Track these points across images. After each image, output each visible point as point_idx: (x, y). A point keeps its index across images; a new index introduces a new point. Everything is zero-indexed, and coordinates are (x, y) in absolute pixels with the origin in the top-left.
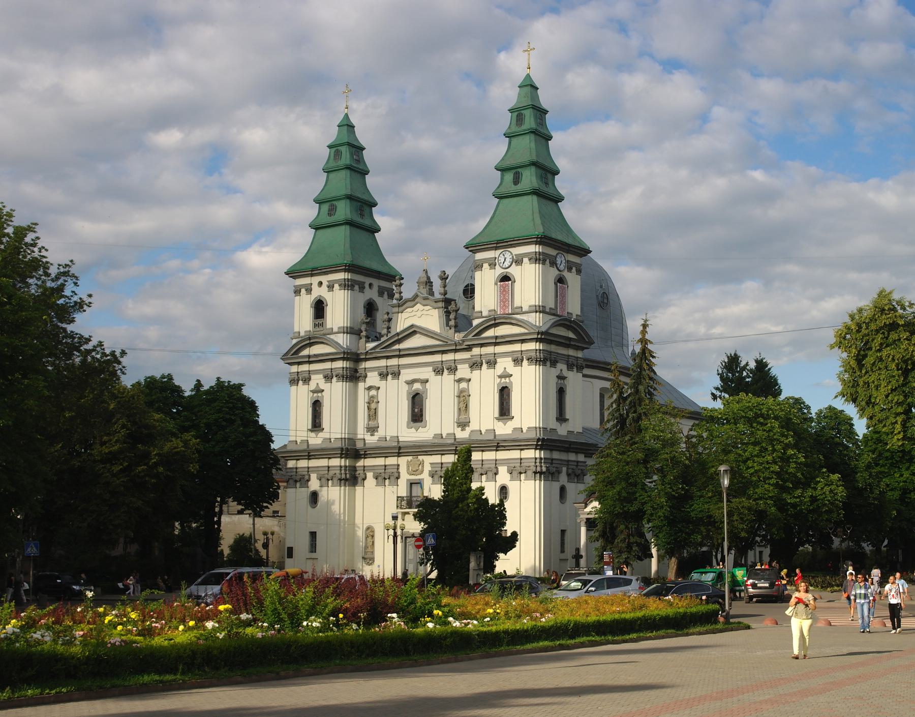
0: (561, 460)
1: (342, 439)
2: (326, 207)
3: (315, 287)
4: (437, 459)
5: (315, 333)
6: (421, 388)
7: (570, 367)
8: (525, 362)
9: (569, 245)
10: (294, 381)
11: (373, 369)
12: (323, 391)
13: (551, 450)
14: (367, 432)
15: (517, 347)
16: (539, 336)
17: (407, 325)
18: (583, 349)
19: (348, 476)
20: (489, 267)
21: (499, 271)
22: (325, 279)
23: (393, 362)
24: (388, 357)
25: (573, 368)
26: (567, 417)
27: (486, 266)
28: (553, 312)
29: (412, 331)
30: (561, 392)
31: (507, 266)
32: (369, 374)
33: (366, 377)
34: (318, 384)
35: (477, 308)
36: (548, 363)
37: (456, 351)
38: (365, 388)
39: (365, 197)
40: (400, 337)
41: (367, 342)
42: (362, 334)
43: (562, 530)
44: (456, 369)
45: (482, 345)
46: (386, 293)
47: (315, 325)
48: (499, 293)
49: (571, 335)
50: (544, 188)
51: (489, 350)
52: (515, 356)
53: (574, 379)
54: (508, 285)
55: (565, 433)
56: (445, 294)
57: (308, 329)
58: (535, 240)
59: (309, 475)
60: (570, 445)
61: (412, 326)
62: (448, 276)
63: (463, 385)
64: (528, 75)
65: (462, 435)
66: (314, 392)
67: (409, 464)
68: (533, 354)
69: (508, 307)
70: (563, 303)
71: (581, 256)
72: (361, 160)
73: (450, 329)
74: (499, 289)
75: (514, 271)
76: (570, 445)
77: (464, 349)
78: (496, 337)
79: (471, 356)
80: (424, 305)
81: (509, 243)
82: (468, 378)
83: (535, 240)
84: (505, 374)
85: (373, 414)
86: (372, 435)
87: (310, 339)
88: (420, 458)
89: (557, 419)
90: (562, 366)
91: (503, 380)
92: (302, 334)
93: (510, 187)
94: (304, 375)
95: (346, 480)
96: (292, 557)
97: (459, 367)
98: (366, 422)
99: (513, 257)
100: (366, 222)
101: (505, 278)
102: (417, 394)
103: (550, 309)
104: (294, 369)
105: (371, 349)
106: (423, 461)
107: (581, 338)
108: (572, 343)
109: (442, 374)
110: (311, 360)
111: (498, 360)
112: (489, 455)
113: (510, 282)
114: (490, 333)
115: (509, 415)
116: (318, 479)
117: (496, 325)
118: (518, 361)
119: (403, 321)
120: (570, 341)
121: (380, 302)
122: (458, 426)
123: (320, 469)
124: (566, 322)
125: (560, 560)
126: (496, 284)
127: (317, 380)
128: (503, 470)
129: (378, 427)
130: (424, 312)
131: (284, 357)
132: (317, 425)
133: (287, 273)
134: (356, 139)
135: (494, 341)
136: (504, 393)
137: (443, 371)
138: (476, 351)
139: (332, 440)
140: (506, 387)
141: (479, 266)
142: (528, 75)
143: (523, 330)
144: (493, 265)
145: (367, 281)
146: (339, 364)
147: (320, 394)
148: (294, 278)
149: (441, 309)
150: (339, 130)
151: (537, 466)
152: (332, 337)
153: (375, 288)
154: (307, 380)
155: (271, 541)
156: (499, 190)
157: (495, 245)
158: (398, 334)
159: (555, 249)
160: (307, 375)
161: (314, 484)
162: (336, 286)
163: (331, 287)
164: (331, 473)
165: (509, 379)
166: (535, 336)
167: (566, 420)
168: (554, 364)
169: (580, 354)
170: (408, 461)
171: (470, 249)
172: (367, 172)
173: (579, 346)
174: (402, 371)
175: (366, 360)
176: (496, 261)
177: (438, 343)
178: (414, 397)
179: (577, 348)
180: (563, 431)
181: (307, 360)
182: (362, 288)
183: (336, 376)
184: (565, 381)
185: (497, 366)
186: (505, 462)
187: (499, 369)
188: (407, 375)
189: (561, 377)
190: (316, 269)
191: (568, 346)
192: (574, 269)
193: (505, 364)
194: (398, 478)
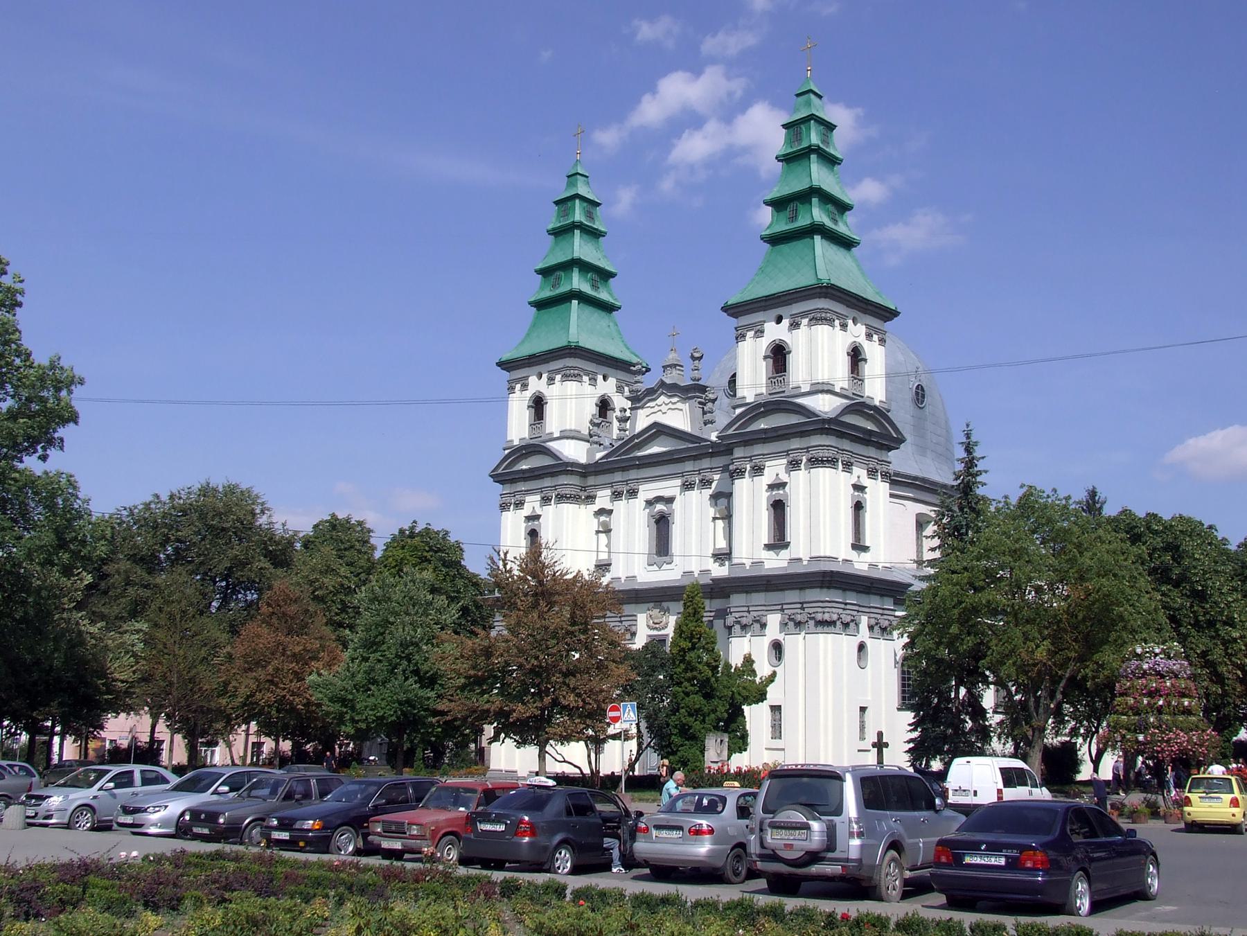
6: (665, 508)
7: (872, 473)
18: (890, 449)
26: (867, 544)
28: (844, 392)
29: (658, 430)
30: (858, 507)
33: (594, 497)
37: (712, 455)
43: (861, 707)
50: (828, 222)
53: (878, 491)
55: (865, 567)
56: (698, 380)
58: (818, 290)
61: (655, 424)
80: (671, 396)
81: (783, 299)
82: (727, 491)
103: (842, 388)
104: (508, 489)
105: (601, 459)
119: (643, 420)
120: (870, 436)
122: (715, 561)
124: (860, 407)
125: (859, 751)
128: (774, 620)
129: (610, 565)
130: (670, 406)
136: (778, 508)
140: (780, 500)
143: (803, 420)
148: (508, 370)
154: (519, 505)
156: (768, 232)
162: (558, 377)
163: (551, 380)
167: (865, 549)
168: (848, 466)
171: (732, 311)
174: (641, 488)
178: (657, 522)
180: (860, 564)
181: (521, 475)
182: (593, 381)
185: (766, 471)
188: (648, 491)
189: (859, 488)
192: (875, 337)
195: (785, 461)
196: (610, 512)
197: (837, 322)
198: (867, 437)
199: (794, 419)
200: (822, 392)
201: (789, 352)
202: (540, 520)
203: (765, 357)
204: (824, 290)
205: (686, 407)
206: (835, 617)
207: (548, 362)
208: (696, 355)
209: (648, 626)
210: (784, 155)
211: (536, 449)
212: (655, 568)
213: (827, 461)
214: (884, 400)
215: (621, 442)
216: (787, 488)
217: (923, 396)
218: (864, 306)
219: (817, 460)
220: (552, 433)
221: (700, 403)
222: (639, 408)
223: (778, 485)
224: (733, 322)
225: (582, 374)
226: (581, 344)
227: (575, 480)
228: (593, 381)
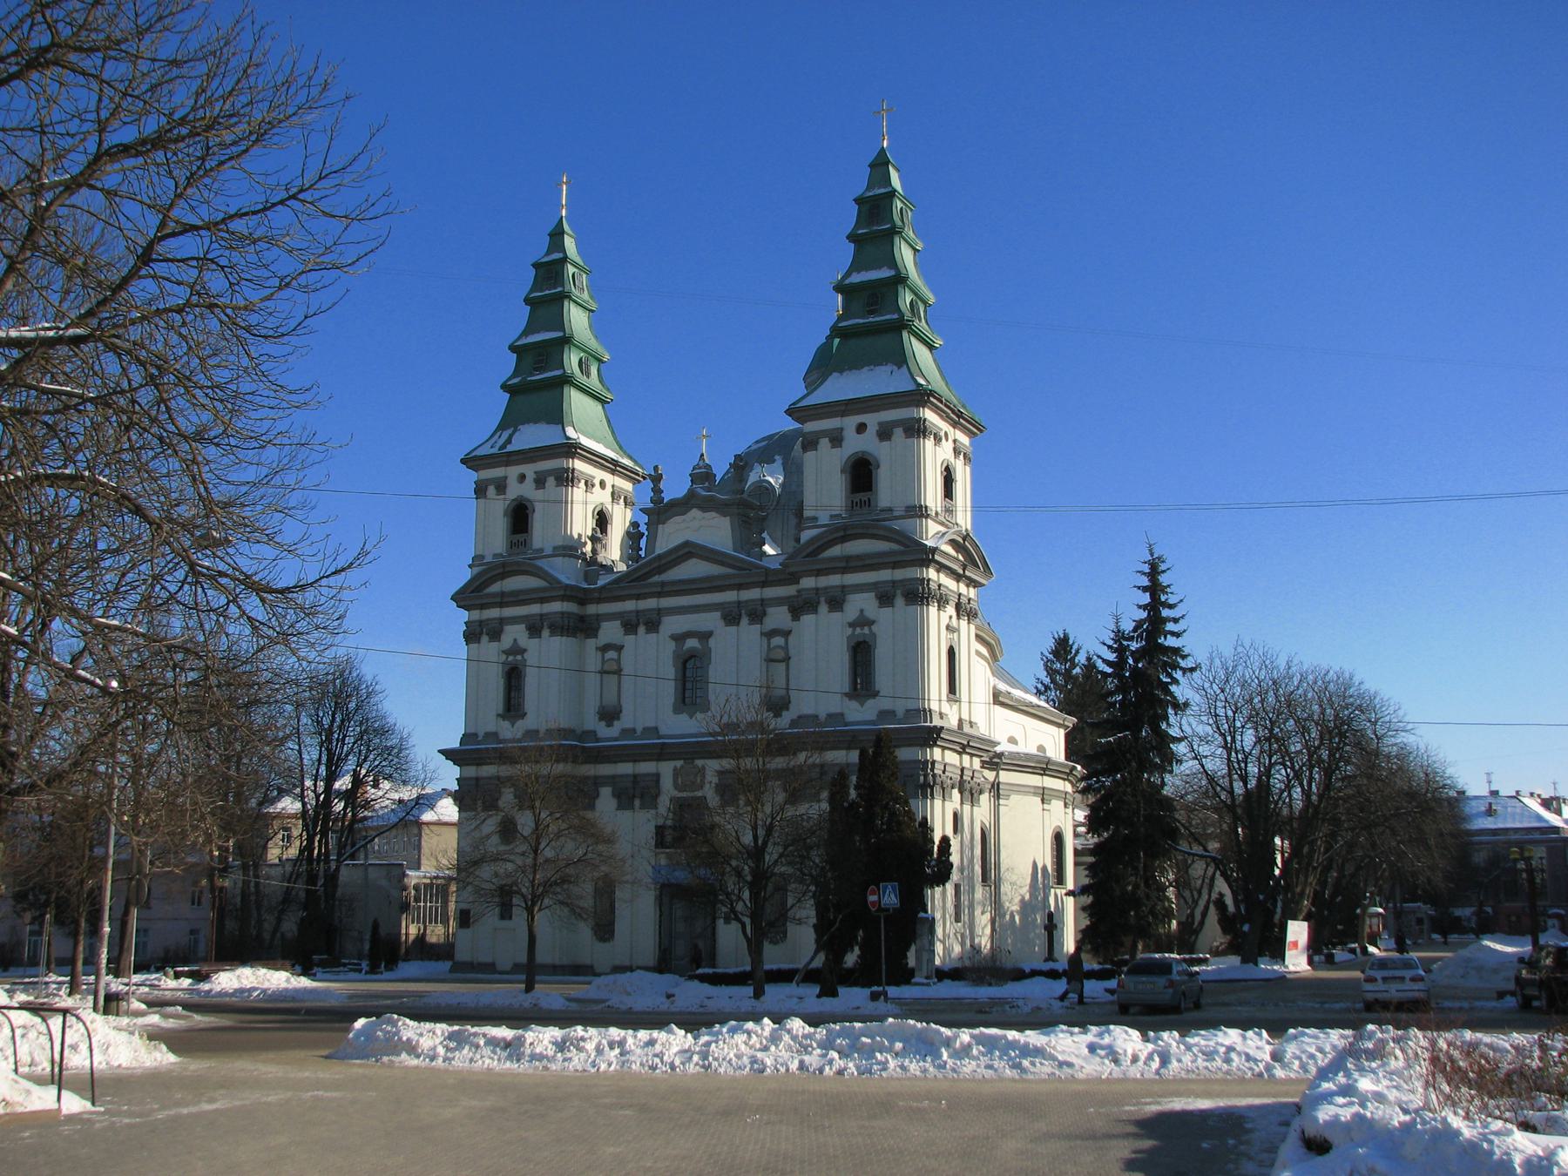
4: (727, 763)
11: (611, 617)
12: (525, 650)
14: (601, 719)
15: (885, 575)
20: (829, 445)
22: (529, 470)
23: (651, 603)
24: (638, 597)
27: (824, 443)
29: (687, 551)
30: (951, 653)
34: (515, 640)
37: (764, 584)
38: (597, 648)
40: (663, 562)
44: (765, 614)
45: (819, 573)
47: (512, 545)
51: (834, 580)
57: (499, 551)
61: (687, 544)
63: (778, 641)
66: (507, 653)
67: (676, 773)
77: (780, 580)
78: (848, 558)
79: (799, 591)
81: (870, 404)
86: (609, 725)
87: (504, 565)
88: (699, 763)
89: (949, 700)
91: (858, 630)
97: (770, 610)
102: (692, 657)
104: (476, 615)
105: (609, 584)
106: (704, 768)
108: (967, 573)
109: (738, 624)
110: (505, 600)
111: (851, 597)
114: (836, 551)
117: (844, 539)
118: (885, 599)
127: (515, 634)
129: (621, 711)
132: (513, 707)
133: (463, 461)
136: (861, 654)
137: (740, 619)
138: (808, 583)
140: (865, 642)
141: (810, 443)
144: (836, 439)
145: (598, 474)
146: (556, 607)
147: (519, 657)
153: (609, 489)
154: (495, 635)
158: (660, 557)
163: (540, 482)
165: (870, 629)
168: (942, 602)
170: (675, 769)
175: (599, 601)
177: (729, 571)
178: (685, 663)
182: (589, 485)
183: (550, 628)
188: (673, 625)
194: (658, 795)
196: (619, 648)
201: (878, 467)
202: (525, 655)
203: (842, 471)
209: (676, 788)
212: (684, 717)
220: (542, 550)
223: (863, 621)
227: (570, 607)
228: (589, 485)
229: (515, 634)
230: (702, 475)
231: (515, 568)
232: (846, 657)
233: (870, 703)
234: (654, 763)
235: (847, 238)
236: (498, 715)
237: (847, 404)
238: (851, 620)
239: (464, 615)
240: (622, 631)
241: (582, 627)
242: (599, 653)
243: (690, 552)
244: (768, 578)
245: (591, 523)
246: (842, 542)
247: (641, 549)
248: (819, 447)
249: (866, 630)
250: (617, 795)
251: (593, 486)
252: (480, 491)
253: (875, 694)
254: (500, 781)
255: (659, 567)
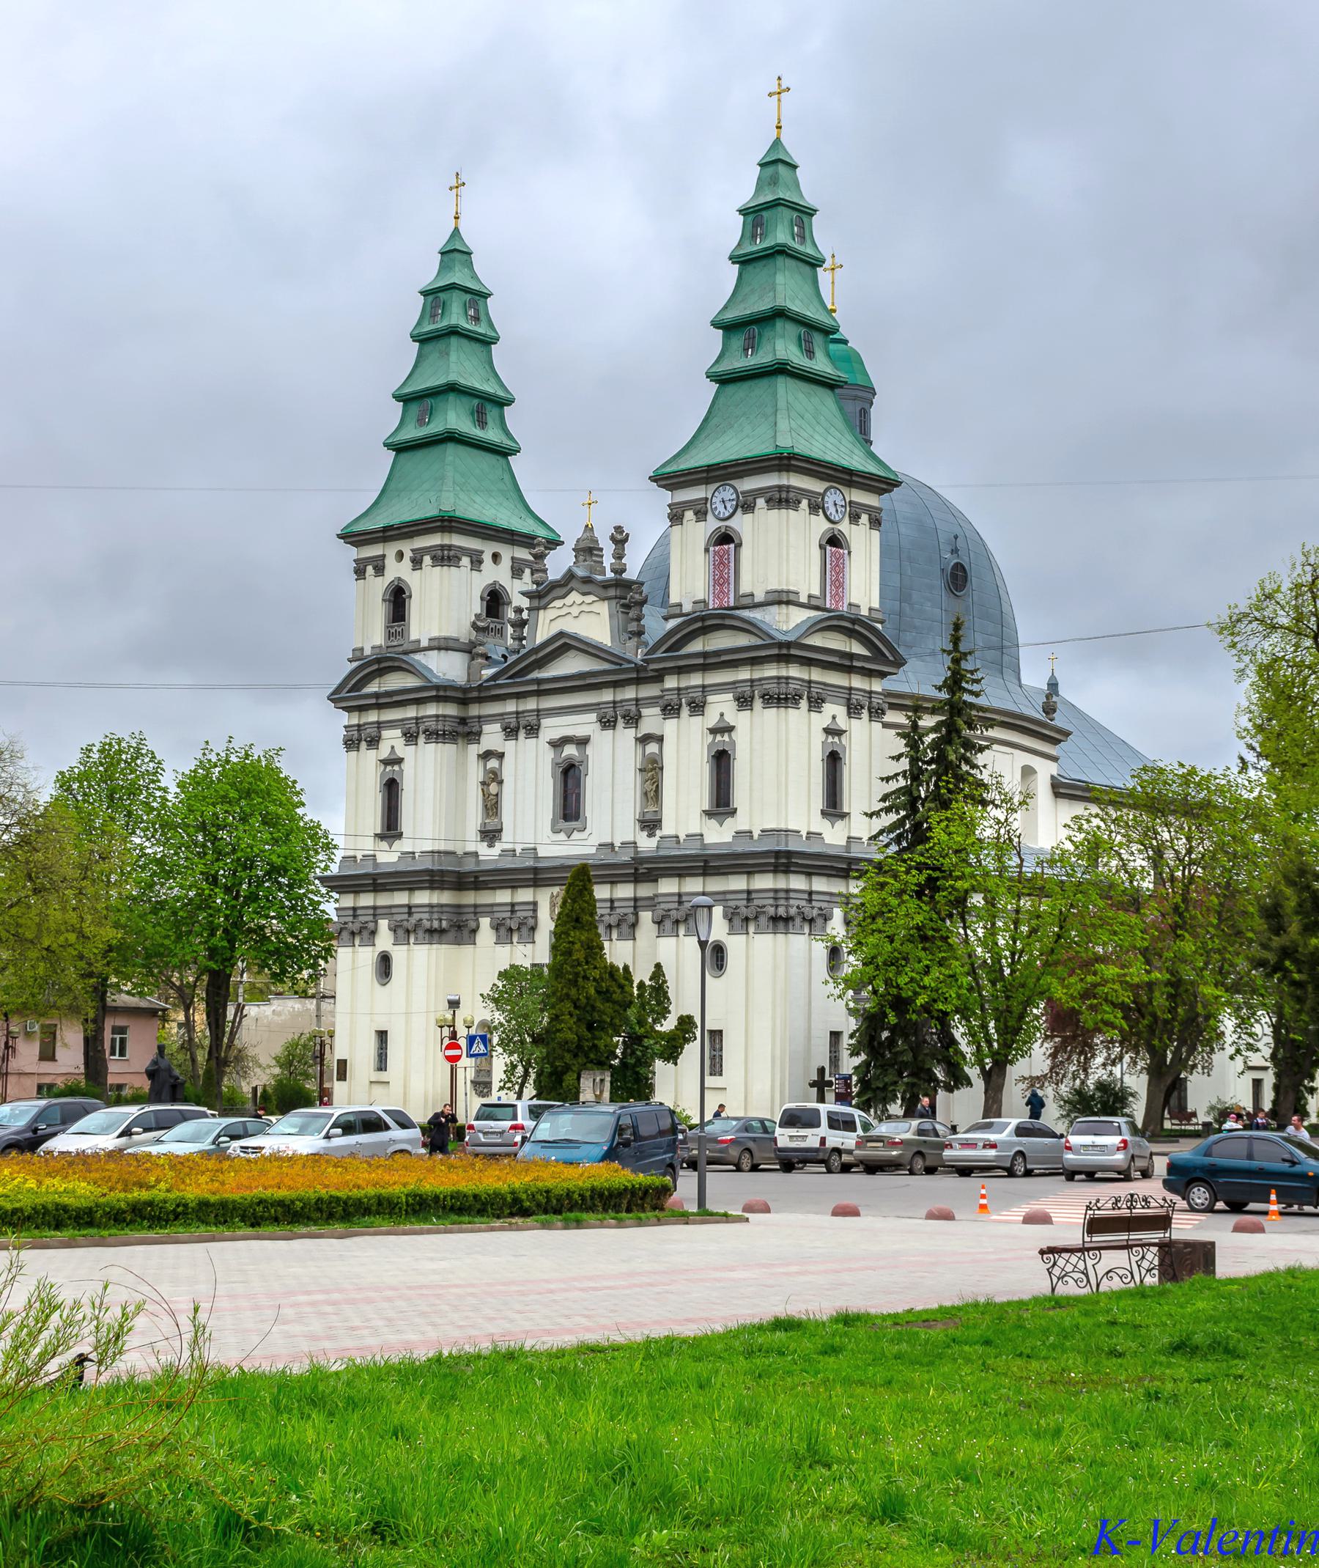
0: (831, 894)
1: (433, 852)
2: (415, 408)
3: (390, 562)
5: (390, 650)
7: (853, 710)
8: (758, 703)
9: (850, 472)
10: (351, 744)
12: (399, 761)
13: (809, 875)
15: (744, 674)
16: (784, 651)
17: (554, 630)
18: (883, 675)
19: (444, 924)
20: (694, 518)
21: (712, 524)
22: (407, 547)
23: (531, 704)
25: (860, 714)
26: (846, 810)
27: (689, 515)
28: (814, 602)
29: (564, 644)
30: (834, 760)
31: (727, 514)
32: (487, 728)
33: (479, 733)
34: (393, 747)
35: (674, 599)
36: (804, 704)
37: (638, 681)
39: (490, 388)
41: (483, 667)
42: (474, 651)
43: (832, 1033)
44: (640, 716)
45: (680, 671)
46: (528, 571)
47: (390, 635)
48: (712, 567)
49: (857, 648)
51: (696, 680)
52: (739, 690)
54: (728, 551)
58: (777, 462)
59: (376, 922)
60: (850, 864)
61: (561, 634)
62: (627, 535)
63: (652, 748)
64: (777, 143)
65: (647, 844)
66: (386, 762)
68: (773, 688)
69: (728, 594)
70: (839, 584)
71: (880, 492)
72: (482, 317)
73: (630, 638)
74: (712, 559)
75: (742, 524)
76: (850, 864)
77: (652, 677)
78: (705, 655)
80: (584, 594)
82: (658, 733)
83: (777, 462)
84: (721, 725)
85: (492, 806)
86: (491, 846)
87: (378, 661)
89: (823, 813)
90: (834, 711)
91: (719, 738)
92: (367, 652)
93: (740, 362)
94: (368, 730)
95: (442, 931)
96: (345, 1079)
97: (645, 712)
98: (480, 821)
99: (738, 497)
100: (492, 434)
101: (725, 538)
103: (810, 596)
105: (487, 681)
107: (878, 655)
108: (856, 664)
109: (614, 726)
110: (382, 701)
111: (710, 699)
112: (693, 885)
113: (732, 546)
114: (696, 646)
115: (728, 805)
116: (390, 929)
117: (705, 630)
119: (545, 627)
121: (517, 591)
122: (642, 829)
123: (394, 910)
126: (707, 550)
127: (392, 740)
129: (501, 830)
131: (336, 697)
132: (391, 828)
133: (341, 537)
134: (475, 277)
135: (701, 661)
136: (722, 761)
137: (615, 722)
138: (671, 682)
139: (417, 855)
142: (777, 143)
145: (488, 548)
146: (431, 710)
147: (396, 768)
149: (614, 602)
150: (442, 261)
151: (777, 906)
152: (418, 657)
153: (506, 563)
154: (374, 742)
155: (327, 1047)
157: (704, 475)
159: (822, 479)
160: (372, 731)
161: (385, 940)
163: (417, 563)
164: (413, 920)
165: (730, 737)
166: (775, 651)
167: (843, 816)
168: (816, 703)
169: (877, 686)
170: (552, 896)
172: (495, 340)
173: (871, 670)
174: (545, 722)
175: (480, 701)
176: (709, 505)
177: (606, 666)
179: (869, 674)
180: (834, 837)
181: (373, 701)
182: (477, 563)
183: (424, 733)
184: (843, 738)
186: (721, 897)
187: (711, 718)
188: (553, 728)
190: (390, 528)
191: (849, 670)
192: (864, 518)
193: (721, 706)
194: (533, 929)
195: (730, 696)
197: (805, 503)
198: (847, 663)
199: (743, 640)
200: (780, 603)
204: (785, 462)
205: (604, 608)
206: (793, 911)
207: (411, 537)
208: (619, 537)
210: (739, 256)
211: (396, 664)
212: (562, 836)
213: (786, 699)
214: (876, 605)
215: (515, 657)
216: (733, 734)
217: (965, 579)
218: (847, 477)
219: (771, 697)
220: (419, 641)
221: (623, 606)
222: (538, 609)
224: (667, 497)
225: (459, 554)
226: (458, 514)
227: (451, 710)
228: (477, 563)
229: (392, 740)
230: (588, 549)
231: (390, 664)
232: (706, 769)
233: (729, 821)
234: (531, 890)
235: (730, 258)
236: (376, 835)
237: (707, 471)
238: (710, 726)
239: (345, 718)
240: (501, 735)
241: (464, 732)
242: (481, 763)
243: (565, 644)
244: (641, 676)
245: (477, 607)
246: (705, 634)
247: (525, 638)
248: (685, 521)
249: (726, 738)
250: (496, 927)
251: (481, 562)
252: (360, 573)
253: (733, 812)
254: (376, 911)
255: (536, 661)
